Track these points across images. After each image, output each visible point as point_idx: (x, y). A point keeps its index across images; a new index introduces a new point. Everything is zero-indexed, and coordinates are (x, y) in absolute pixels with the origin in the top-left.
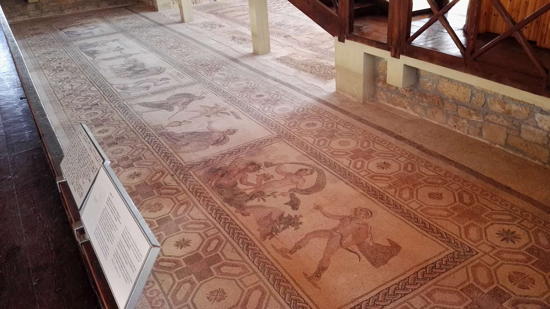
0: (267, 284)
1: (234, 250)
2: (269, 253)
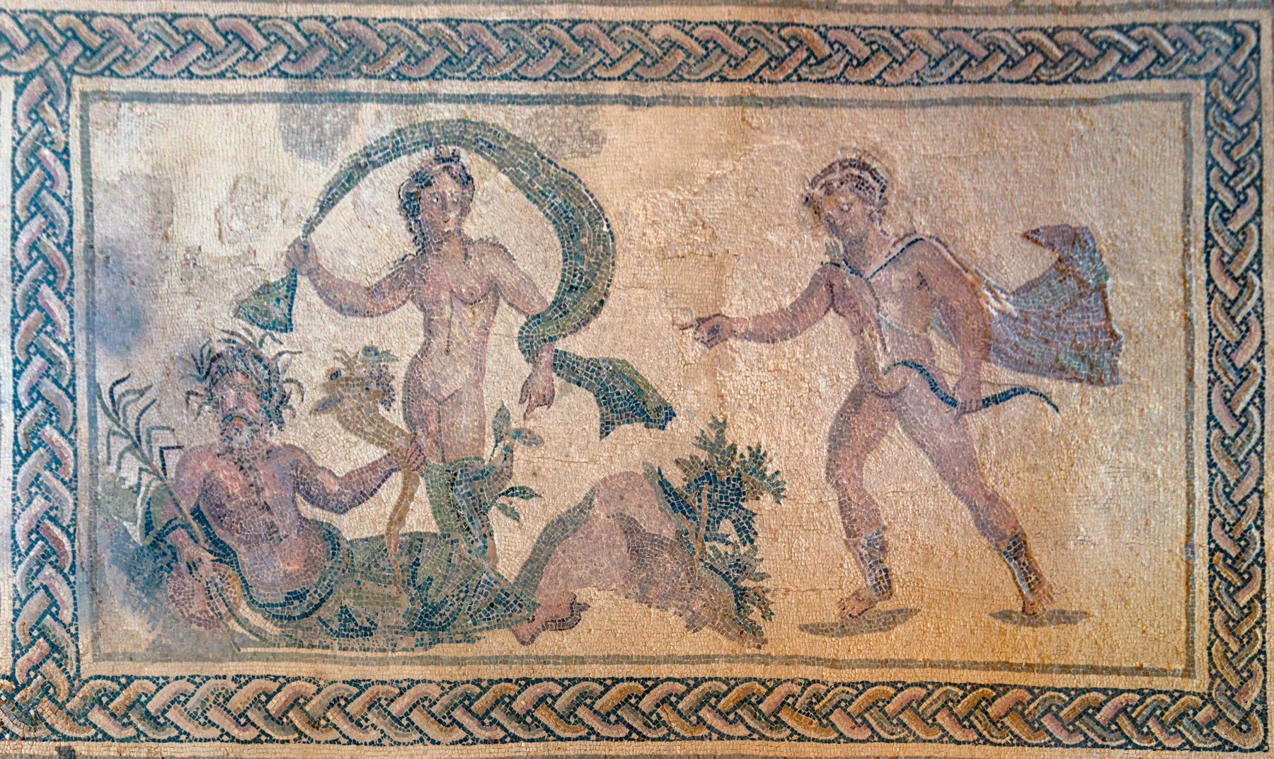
2: (834, 664)
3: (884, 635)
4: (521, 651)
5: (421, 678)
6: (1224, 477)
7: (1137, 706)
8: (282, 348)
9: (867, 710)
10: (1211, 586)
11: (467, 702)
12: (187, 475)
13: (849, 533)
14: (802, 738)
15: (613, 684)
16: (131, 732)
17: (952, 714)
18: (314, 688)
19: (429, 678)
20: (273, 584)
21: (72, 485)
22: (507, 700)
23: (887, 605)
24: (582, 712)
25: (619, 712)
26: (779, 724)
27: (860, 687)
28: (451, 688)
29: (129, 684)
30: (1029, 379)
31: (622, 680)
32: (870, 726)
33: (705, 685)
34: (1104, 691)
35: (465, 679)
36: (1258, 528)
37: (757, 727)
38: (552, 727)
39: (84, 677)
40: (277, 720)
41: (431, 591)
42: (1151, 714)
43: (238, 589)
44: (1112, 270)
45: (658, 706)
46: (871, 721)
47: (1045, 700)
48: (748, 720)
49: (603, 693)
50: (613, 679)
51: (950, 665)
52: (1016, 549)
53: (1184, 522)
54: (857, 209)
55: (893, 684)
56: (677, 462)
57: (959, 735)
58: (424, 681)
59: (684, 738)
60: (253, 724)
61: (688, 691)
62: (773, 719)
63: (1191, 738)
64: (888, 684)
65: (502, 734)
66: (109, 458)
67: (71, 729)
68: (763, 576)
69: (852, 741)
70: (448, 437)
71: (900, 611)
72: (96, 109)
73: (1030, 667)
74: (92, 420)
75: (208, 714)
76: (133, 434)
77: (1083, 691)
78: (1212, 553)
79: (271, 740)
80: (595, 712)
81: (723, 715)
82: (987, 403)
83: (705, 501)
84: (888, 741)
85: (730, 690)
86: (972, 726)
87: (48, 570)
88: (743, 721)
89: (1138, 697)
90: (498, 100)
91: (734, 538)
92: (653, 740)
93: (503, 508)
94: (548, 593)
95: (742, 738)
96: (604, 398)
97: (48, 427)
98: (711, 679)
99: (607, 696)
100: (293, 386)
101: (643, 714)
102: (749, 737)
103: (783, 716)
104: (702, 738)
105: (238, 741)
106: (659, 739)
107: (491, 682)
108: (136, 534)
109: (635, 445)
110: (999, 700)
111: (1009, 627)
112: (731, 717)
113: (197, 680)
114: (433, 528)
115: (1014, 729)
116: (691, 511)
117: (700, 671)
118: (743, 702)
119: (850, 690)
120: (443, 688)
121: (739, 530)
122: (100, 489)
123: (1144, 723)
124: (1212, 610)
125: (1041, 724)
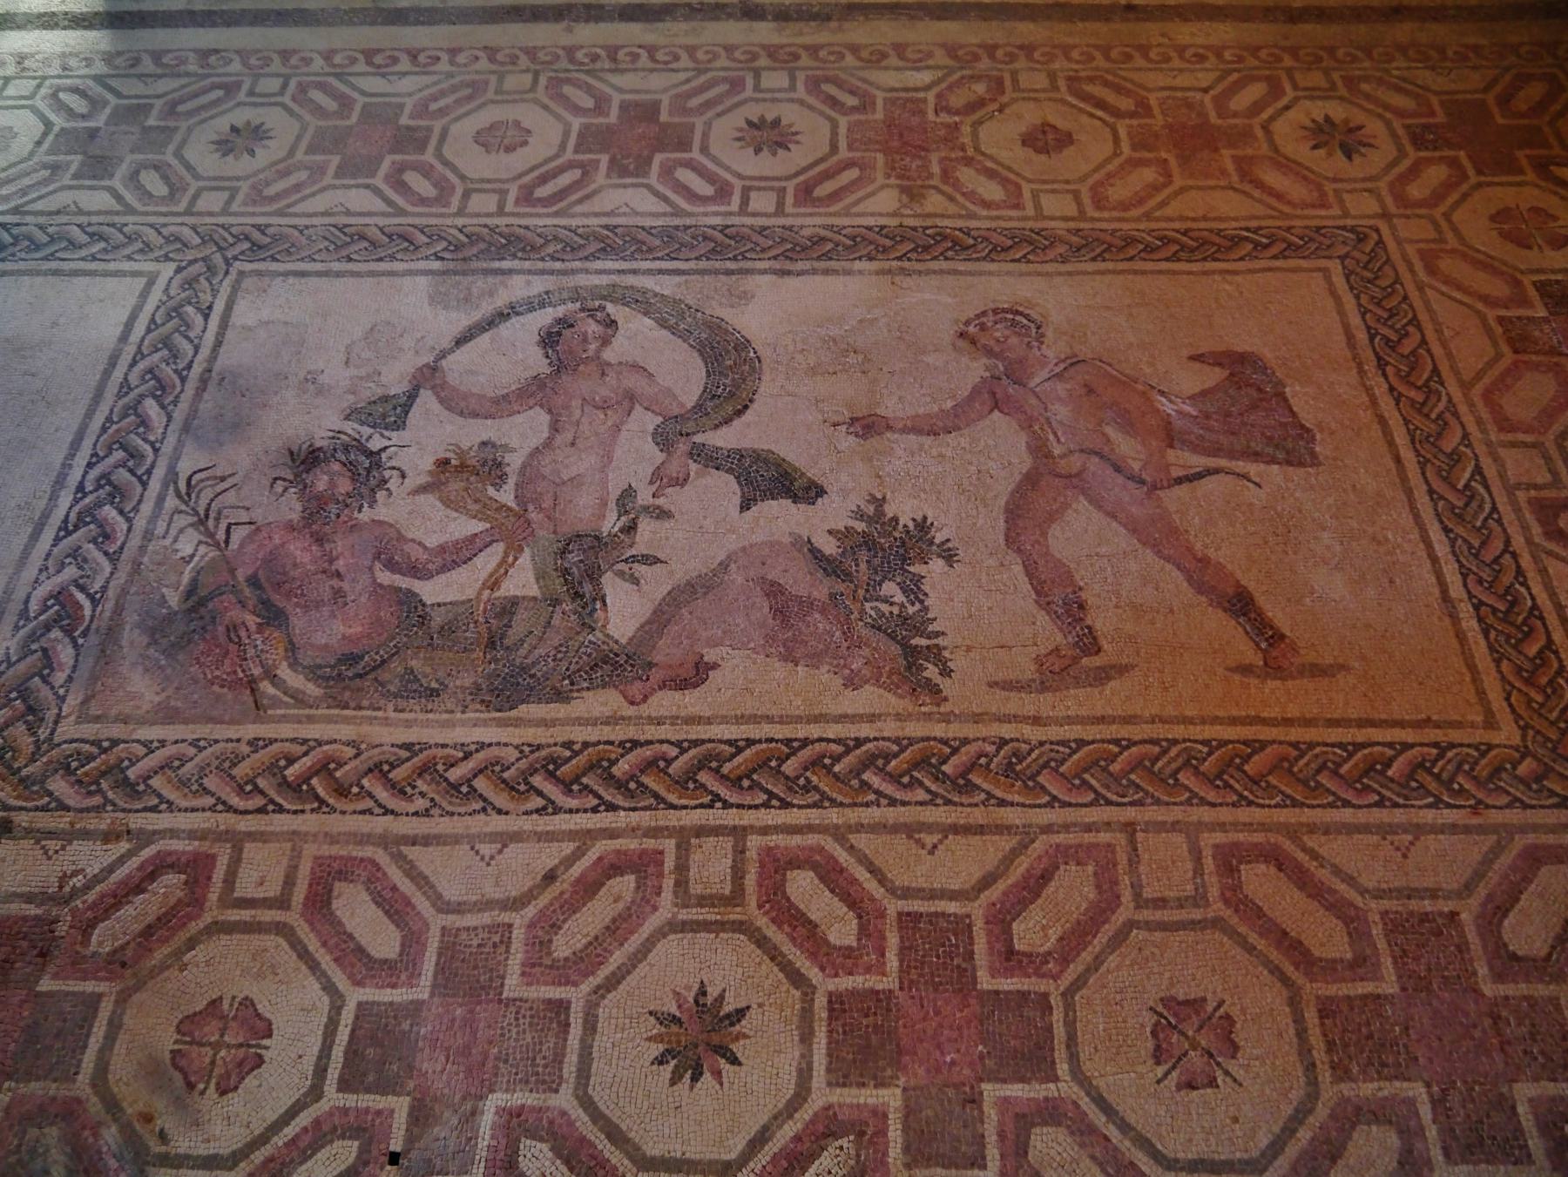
0: (1231, 821)
1: (929, 840)
2: (1036, 721)
3: (1096, 691)
4: (630, 711)
5: (494, 741)
6: (1465, 540)
7: (1436, 760)
8: (387, 443)
9: (1086, 770)
10: (1487, 637)
11: (551, 767)
12: (250, 548)
13: (1038, 593)
14: (1002, 803)
15: (748, 746)
16: (97, 800)
17: (1197, 772)
18: (355, 751)
19: (504, 740)
20: (326, 645)
21: (113, 558)
22: (605, 764)
23: (1096, 661)
24: (703, 777)
25: (755, 777)
26: (970, 788)
27: (1073, 745)
28: (532, 752)
29: (111, 748)
30: (1223, 462)
31: (760, 741)
32: (1091, 788)
33: (870, 746)
34: (1391, 745)
35: (551, 741)
36: (1522, 584)
37: (941, 791)
38: (663, 792)
39: (56, 740)
40: (295, 788)
41: (522, 652)
42: (1459, 767)
43: (281, 651)
44: (1289, 381)
45: (806, 769)
46: (1093, 782)
47: (1317, 756)
48: (927, 783)
49: (733, 756)
50: (747, 740)
51: (1188, 721)
52: (1241, 605)
53: (1434, 580)
54: (1014, 340)
55: (1117, 742)
56: (830, 532)
57: (1211, 796)
58: (498, 744)
59: (841, 804)
60: (262, 792)
61: (848, 751)
62: (961, 782)
63: (1519, 795)
64: (1109, 742)
65: (596, 802)
66: (167, 532)
67: (17, 798)
68: (937, 634)
69: (1070, 805)
70: (563, 512)
71: (1113, 667)
72: (248, 283)
73: (1288, 722)
74: (161, 499)
75: (205, 781)
76: (202, 513)
77: (1363, 746)
78: (1477, 608)
79: (280, 809)
80: (723, 776)
81: (895, 778)
82: (1179, 481)
83: (863, 566)
84: (1118, 804)
85: (902, 751)
86: (1227, 785)
87: (56, 633)
88: (921, 784)
89: (1435, 751)
90: (649, 272)
91: (899, 597)
92: (800, 807)
93: (621, 574)
94: (666, 651)
95: (921, 804)
96: (744, 479)
97: (107, 507)
98: (876, 739)
99: (739, 759)
100: (395, 473)
101: (787, 778)
102: (931, 803)
103: (976, 779)
104: (867, 805)
105: (236, 811)
106: (808, 806)
107: (586, 745)
108: (174, 600)
109: (781, 518)
110: (1256, 758)
111: (1253, 681)
112: (906, 780)
113: (202, 743)
114: (534, 591)
115: (1283, 788)
116: (849, 574)
117: (865, 730)
118: (921, 763)
119: (1061, 749)
120: (522, 752)
121: (904, 591)
122: (145, 559)
123: (1452, 780)
124: (1498, 662)
125: (1317, 782)
